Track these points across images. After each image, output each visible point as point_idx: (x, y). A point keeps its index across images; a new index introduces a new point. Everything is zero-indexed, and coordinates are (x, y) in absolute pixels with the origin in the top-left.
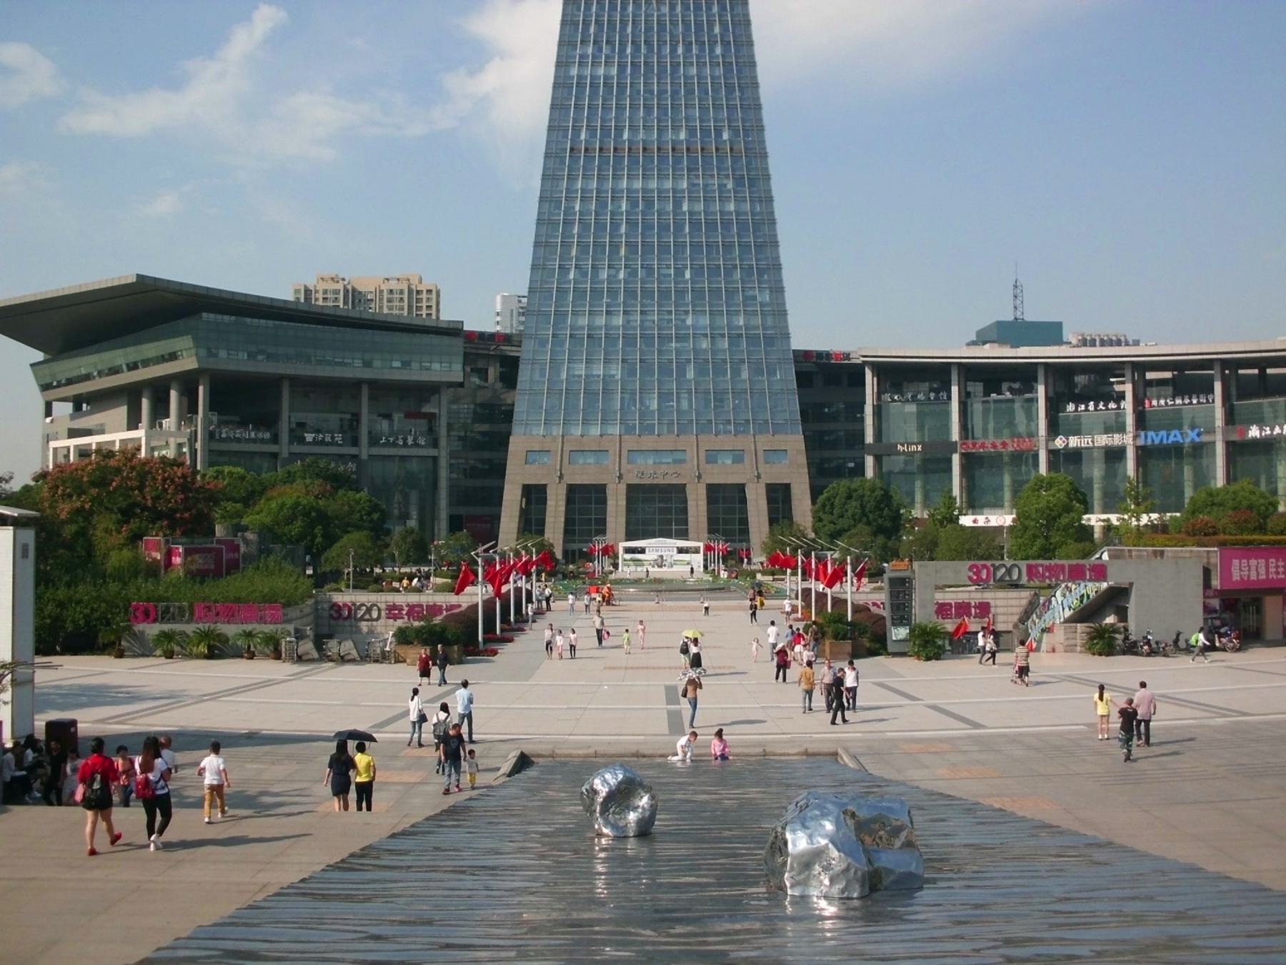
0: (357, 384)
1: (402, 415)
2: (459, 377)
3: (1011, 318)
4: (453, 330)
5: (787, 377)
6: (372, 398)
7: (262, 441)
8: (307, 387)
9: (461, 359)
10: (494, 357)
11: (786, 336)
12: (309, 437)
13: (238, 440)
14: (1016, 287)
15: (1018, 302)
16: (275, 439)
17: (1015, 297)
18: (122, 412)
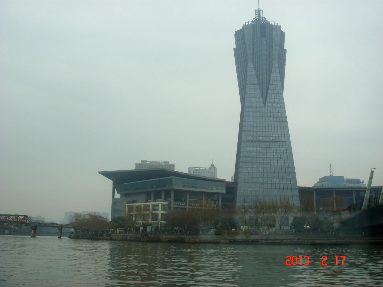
0: (202, 192)
1: (210, 200)
2: (224, 192)
3: (329, 175)
4: (223, 181)
5: (296, 193)
6: (189, 195)
7: (183, 205)
8: (192, 193)
9: (225, 188)
10: (231, 188)
11: (296, 183)
12: (192, 204)
13: (179, 205)
14: (330, 166)
15: (331, 171)
16: (186, 205)
17: (330, 169)
18: (144, 197)
